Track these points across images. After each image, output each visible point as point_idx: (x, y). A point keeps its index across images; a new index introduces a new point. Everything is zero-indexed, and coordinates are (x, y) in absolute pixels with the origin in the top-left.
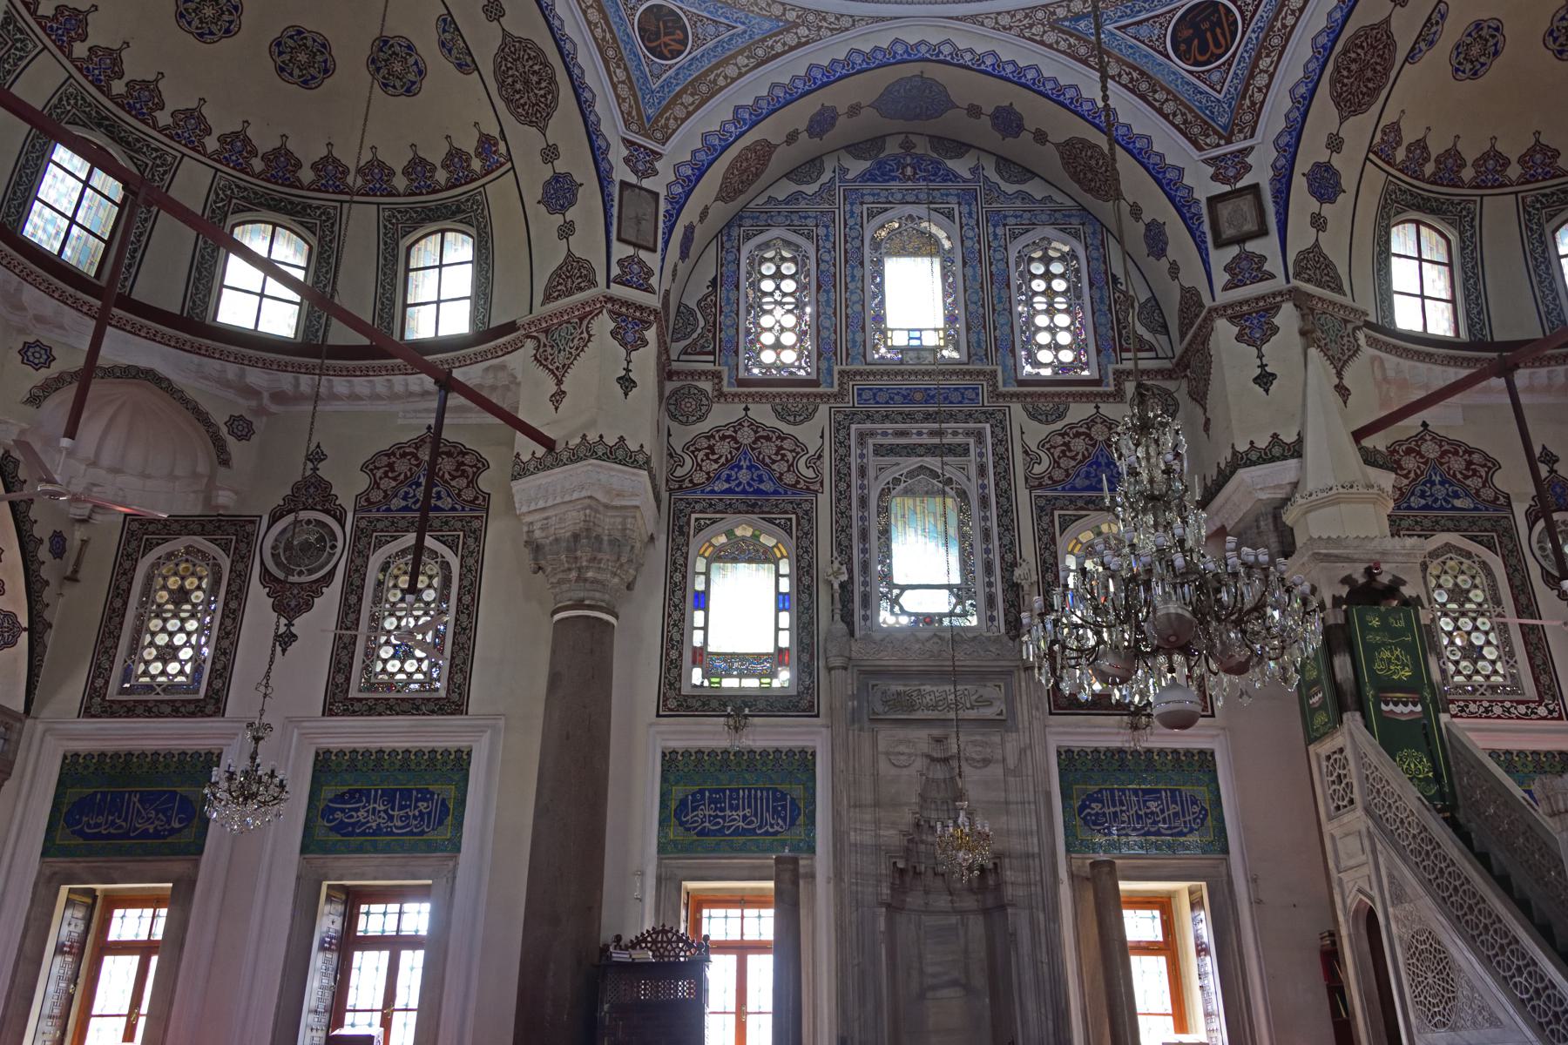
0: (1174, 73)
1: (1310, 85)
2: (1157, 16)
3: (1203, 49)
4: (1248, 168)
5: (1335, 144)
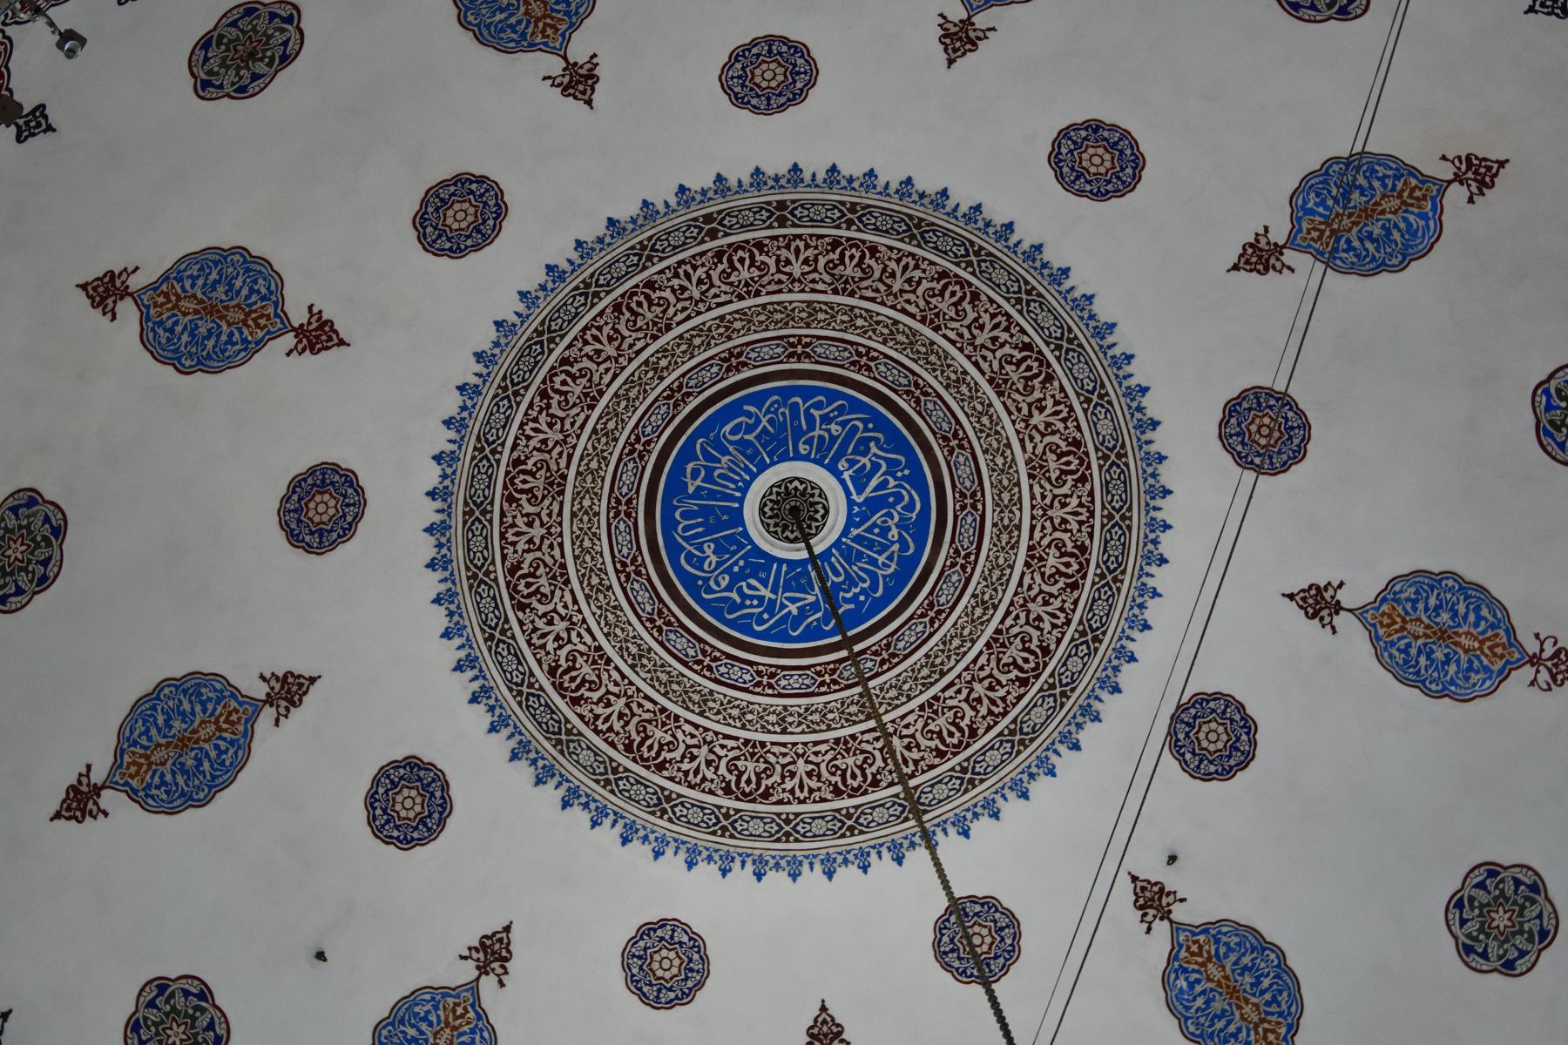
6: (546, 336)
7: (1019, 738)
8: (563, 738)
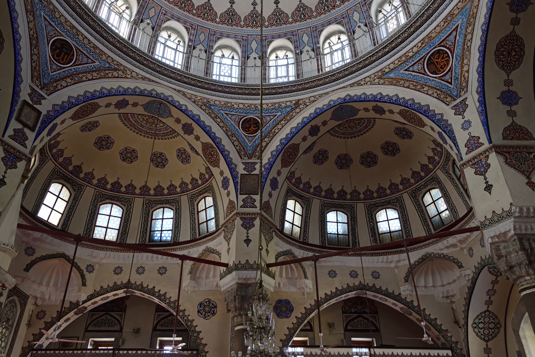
0: (45, 51)
1: (77, 103)
2: (57, 30)
3: (59, 55)
4: (41, 104)
5: (63, 122)
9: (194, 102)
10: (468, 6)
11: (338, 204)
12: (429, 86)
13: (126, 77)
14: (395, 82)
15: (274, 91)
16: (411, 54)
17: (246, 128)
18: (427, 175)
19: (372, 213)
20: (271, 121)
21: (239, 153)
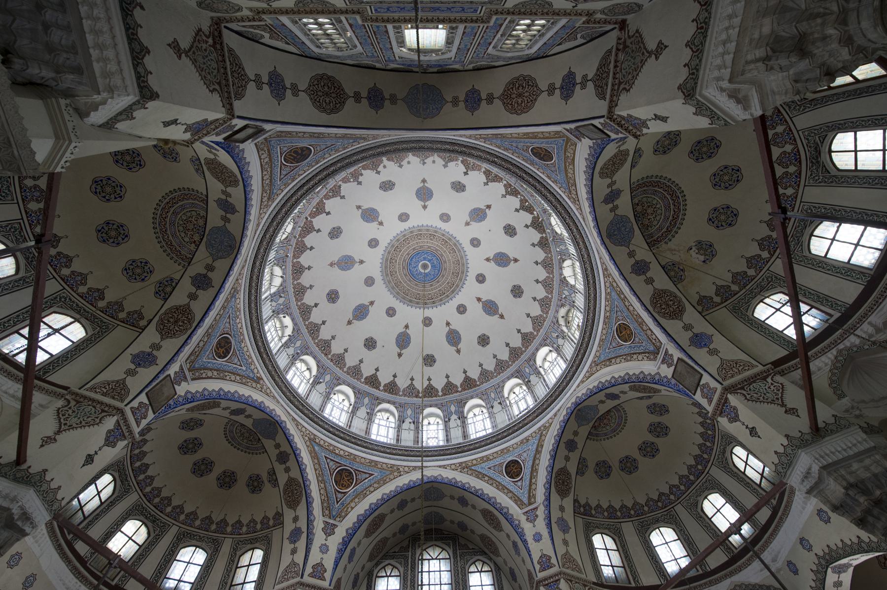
6: (453, 292)
7: (398, 240)
8: (455, 245)
9: (237, 280)
10: (388, 473)
11: (126, 475)
12: (325, 486)
13: (261, 208)
14: (314, 455)
15: (262, 350)
16: (337, 452)
17: (220, 344)
18: (215, 532)
19: (130, 515)
20: (235, 366)
21: (191, 354)
